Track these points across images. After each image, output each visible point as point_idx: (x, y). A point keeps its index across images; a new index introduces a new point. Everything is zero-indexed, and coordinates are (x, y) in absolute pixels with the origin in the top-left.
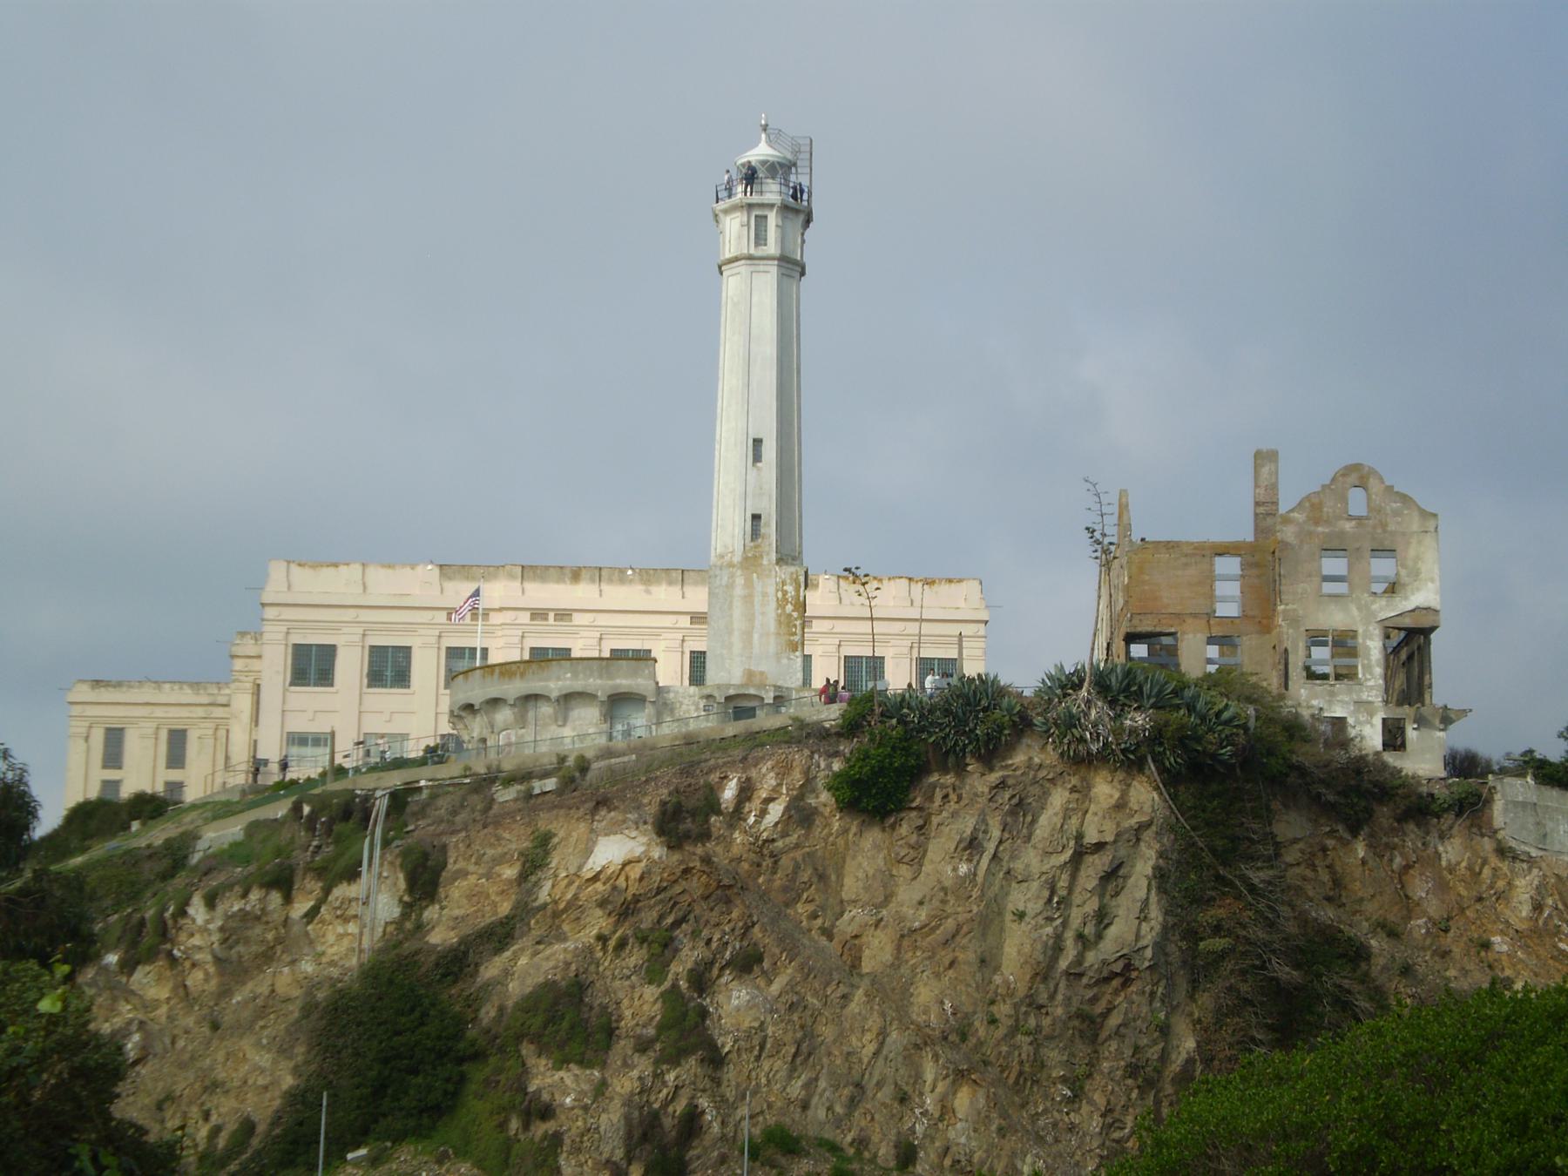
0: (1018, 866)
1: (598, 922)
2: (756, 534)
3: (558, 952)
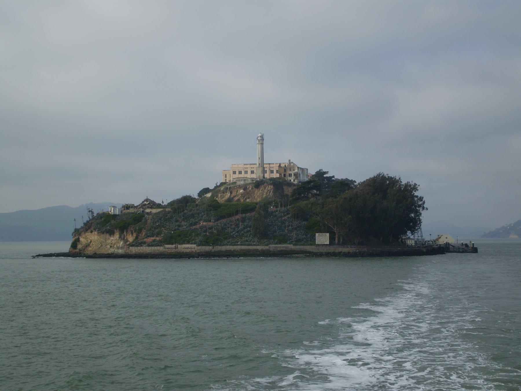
0: (265, 191)
1: (240, 195)
2: (259, 165)
3: (238, 198)
